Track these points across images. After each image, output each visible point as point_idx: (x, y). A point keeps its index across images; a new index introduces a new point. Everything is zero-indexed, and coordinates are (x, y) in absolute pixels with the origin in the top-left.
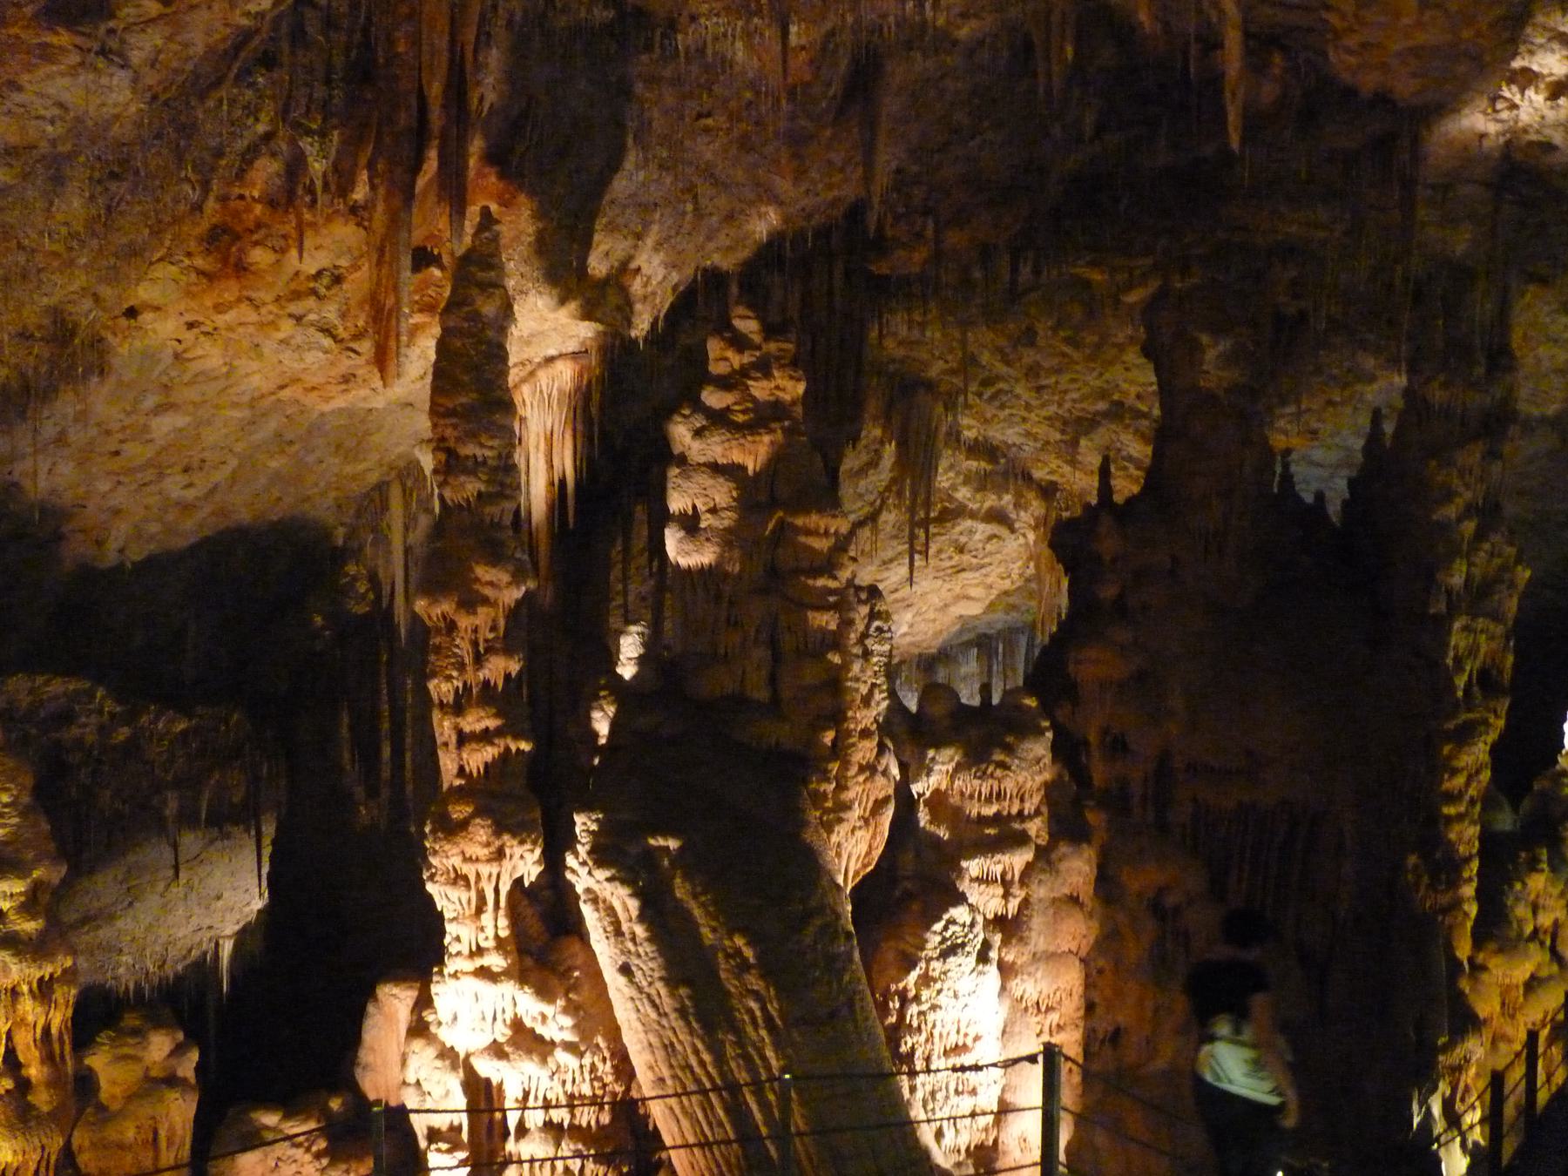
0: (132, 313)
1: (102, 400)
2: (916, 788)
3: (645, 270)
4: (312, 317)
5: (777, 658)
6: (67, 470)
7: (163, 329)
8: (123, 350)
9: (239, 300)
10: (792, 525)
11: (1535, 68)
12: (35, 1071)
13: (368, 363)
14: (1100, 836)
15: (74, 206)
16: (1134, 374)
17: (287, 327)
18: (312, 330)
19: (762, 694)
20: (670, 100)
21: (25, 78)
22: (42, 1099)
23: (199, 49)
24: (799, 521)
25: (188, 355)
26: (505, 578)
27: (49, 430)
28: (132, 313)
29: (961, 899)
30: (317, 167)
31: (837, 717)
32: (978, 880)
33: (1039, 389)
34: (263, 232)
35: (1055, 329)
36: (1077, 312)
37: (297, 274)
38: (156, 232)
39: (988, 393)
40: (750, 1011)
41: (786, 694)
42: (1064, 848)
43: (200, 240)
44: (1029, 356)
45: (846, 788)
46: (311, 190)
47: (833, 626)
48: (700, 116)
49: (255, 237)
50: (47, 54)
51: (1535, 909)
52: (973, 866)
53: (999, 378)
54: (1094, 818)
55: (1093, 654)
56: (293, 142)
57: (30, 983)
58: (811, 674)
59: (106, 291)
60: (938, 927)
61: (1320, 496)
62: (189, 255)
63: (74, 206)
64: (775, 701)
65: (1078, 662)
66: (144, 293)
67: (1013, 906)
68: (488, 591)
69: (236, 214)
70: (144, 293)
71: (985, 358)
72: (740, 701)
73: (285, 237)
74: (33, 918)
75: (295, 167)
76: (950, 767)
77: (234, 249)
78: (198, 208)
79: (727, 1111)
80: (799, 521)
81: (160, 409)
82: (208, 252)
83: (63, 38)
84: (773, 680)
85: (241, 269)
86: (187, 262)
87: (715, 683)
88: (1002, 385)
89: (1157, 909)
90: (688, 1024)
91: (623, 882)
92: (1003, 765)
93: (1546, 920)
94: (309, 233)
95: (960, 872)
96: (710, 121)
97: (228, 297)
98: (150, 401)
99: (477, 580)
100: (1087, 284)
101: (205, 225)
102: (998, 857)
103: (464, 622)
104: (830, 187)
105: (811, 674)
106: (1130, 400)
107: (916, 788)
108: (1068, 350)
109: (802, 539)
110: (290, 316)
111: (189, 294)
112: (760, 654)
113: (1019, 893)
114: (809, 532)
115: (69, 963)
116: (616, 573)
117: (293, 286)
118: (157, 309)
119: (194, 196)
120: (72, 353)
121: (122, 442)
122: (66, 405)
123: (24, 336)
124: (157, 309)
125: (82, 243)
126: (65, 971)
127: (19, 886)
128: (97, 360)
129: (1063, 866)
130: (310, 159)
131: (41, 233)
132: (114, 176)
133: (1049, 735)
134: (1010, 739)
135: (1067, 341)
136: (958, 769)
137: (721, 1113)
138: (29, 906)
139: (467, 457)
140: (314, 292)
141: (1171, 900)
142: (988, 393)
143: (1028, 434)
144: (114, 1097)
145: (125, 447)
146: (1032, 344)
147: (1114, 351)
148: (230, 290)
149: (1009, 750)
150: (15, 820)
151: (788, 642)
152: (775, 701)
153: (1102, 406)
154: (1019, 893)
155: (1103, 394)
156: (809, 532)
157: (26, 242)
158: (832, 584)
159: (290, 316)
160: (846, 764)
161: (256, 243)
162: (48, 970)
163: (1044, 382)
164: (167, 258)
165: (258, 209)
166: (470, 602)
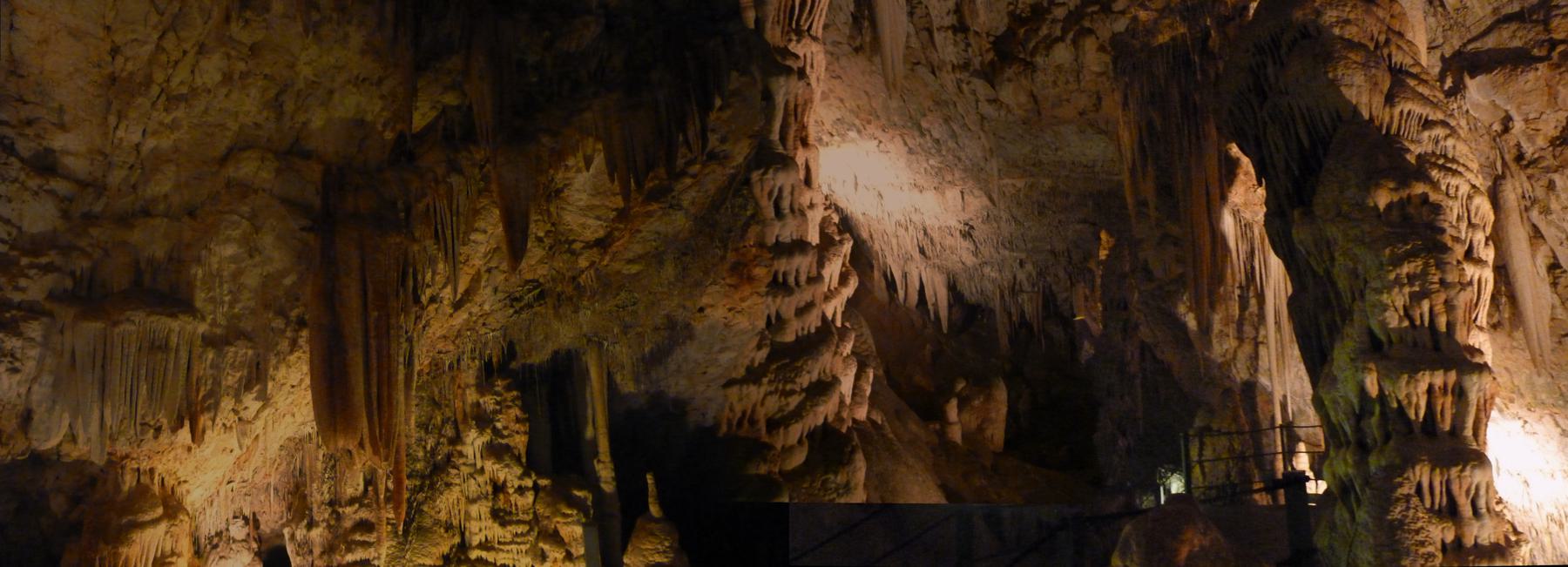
0: (701, 310)
1: (692, 351)
6: (683, 382)
7: (718, 314)
8: (699, 327)
15: (669, 271)
21: (642, 227)
23: (712, 192)
27: (673, 367)
28: (701, 310)
38: (706, 273)
50: (649, 214)
59: (688, 304)
63: (669, 271)
66: (705, 300)
70: (705, 300)
78: (723, 258)
81: (722, 351)
83: (655, 206)
85: (751, 279)
98: (716, 348)
101: (727, 266)
111: (727, 296)
120: (677, 333)
122: (678, 355)
123: (656, 329)
128: (688, 333)
132: (685, 254)
148: (747, 290)
164: (714, 283)
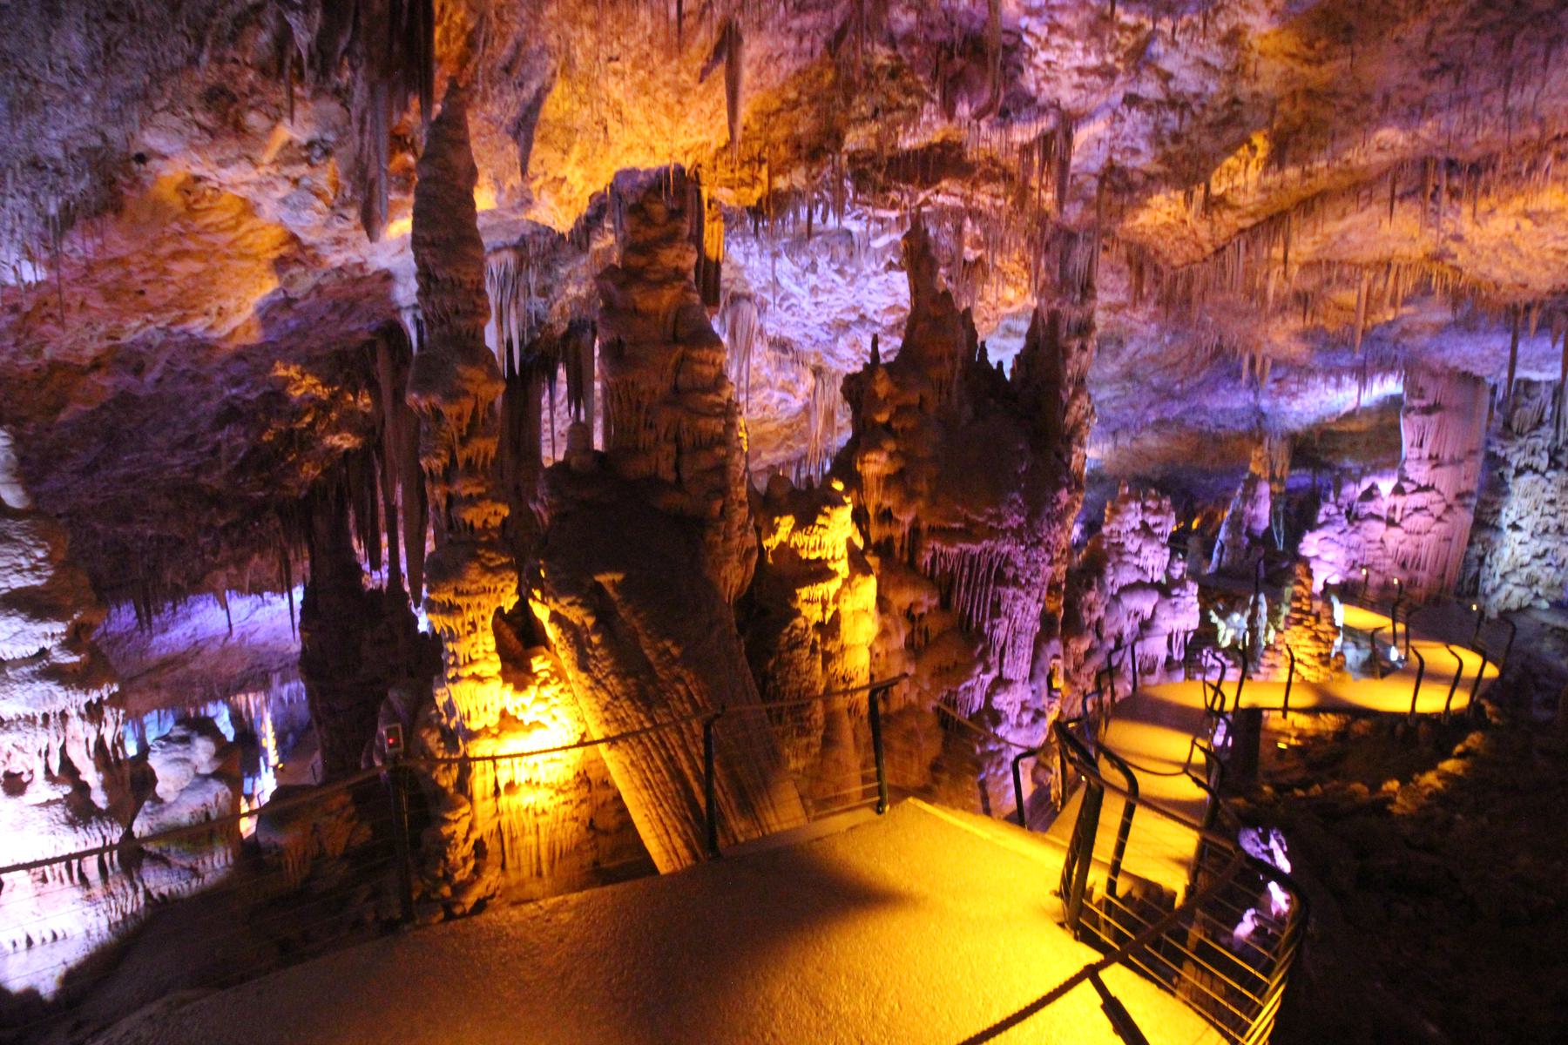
2: (766, 543)
3: (570, 179)
4: (305, 182)
5: (679, 452)
9: (240, 157)
10: (692, 359)
11: (1140, 93)
12: (91, 775)
13: (356, 228)
14: (876, 571)
16: (874, 297)
17: (284, 189)
18: (306, 193)
19: (672, 477)
20: (589, 41)
22: (99, 798)
24: (695, 354)
25: (197, 206)
26: (482, 376)
29: (798, 613)
30: (303, 39)
31: (723, 491)
32: (807, 601)
33: (816, 304)
34: (257, 98)
35: (831, 260)
36: (842, 252)
37: (290, 143)
39: (786, 304)
40: (677, 692)
41: (686, 476)
42: (859, 578)
43: (200, 98)
44: (812, 279)
45: (730, 539)
46: (297, 63)
47: (720, 429)
48: (610, 59)
49: (251, 102)
51: (1090, 610)
52: (804, 593)
53: (792, 295)
54: (873, 561)
55: (872, 456)
56: (280, 17)
57: (78, 707)
58: (705, 461)
60: (787, 630)
61: (1000, 364)
62: (191, 109)
64: (679, 479)
65: (862, 462)
67: (829, 615)
68: (468, 386)
69: (232, 77)
71: (784, 281)
72: (654, 481)
73: (277, 106)
74: (77, 653)
75: (284, 38)
76: (789, 529)
77: (232, 110)
79: (664, 762)
80: (695, 354)
82: (209, 110)
84: (677, 468)
86: (188, 115)
87: (639, 467)
88: (793, 301)
89: (909, 615)
90: (633, 703)
91: (582, 606)
92: (823, 526)
93: (1095, 617)
94: (298, 105)
95: (795, 597)
96: (618, 65)
97: (230, 153)
99: (459, 376)
100: (849, 233)
102: (820, 585)
103: (449, 410)
104: (700, 132)
105: (705, 461)
106: (870, 314)
107: (766, 543)
108: (837, 278)
109: (697, 368)
110: (287, 178)
112: (670, 448)
113: (832, 608)
114: (701, 362)
115: (116, 689)
116: (545, 415)
117: (287, 153)
118: (164, 157)
119: (190, 48)
121: (146, 282)
124: (164, 157)
125: (85, 81)
126: (111, 697)
127: (59, 628)
129: (860, 590)
130: (295, 31)
131: (42, 65)
133: (850, 508)
134: (827, 509)
135: (840, 272)
136: (793, 530)
137: (659, 763)
138: (69, 644)
139: (445, 280)
140: (307, 160)
141: (918, 611)
142: (786, 304)
143: (806, 335)
144: (167, 791)
145: (147, 288)
146: (815, 272)
147: (863, 281)
149: (827, 515)
150: (50, 573)
151: (687, 440)
152: (679, 479)
153: (854, 317)
154: (832, 608)
155: (854, 309)
156: (701, 362)
157: (27, 71)
158: (718, 400)
159: (287, 178)
160: (729, 526)
161: (252, 108)
162: (94, 696)
163: (820, 299)
165: (251, 75)
166: (453, 396)
